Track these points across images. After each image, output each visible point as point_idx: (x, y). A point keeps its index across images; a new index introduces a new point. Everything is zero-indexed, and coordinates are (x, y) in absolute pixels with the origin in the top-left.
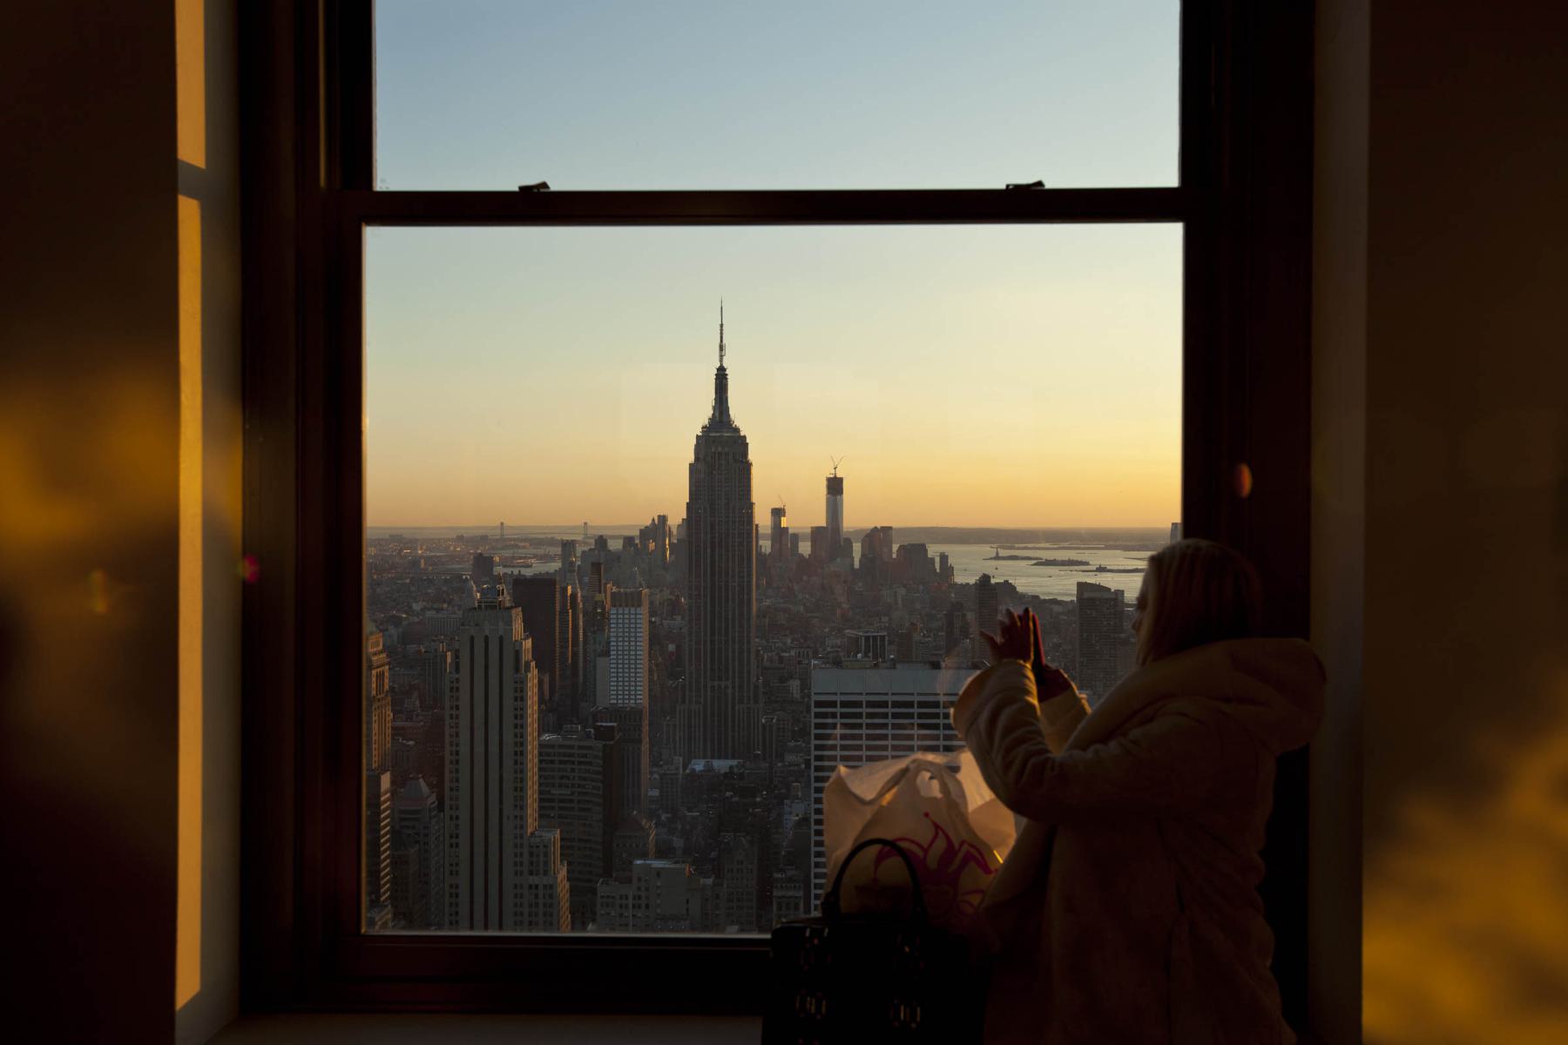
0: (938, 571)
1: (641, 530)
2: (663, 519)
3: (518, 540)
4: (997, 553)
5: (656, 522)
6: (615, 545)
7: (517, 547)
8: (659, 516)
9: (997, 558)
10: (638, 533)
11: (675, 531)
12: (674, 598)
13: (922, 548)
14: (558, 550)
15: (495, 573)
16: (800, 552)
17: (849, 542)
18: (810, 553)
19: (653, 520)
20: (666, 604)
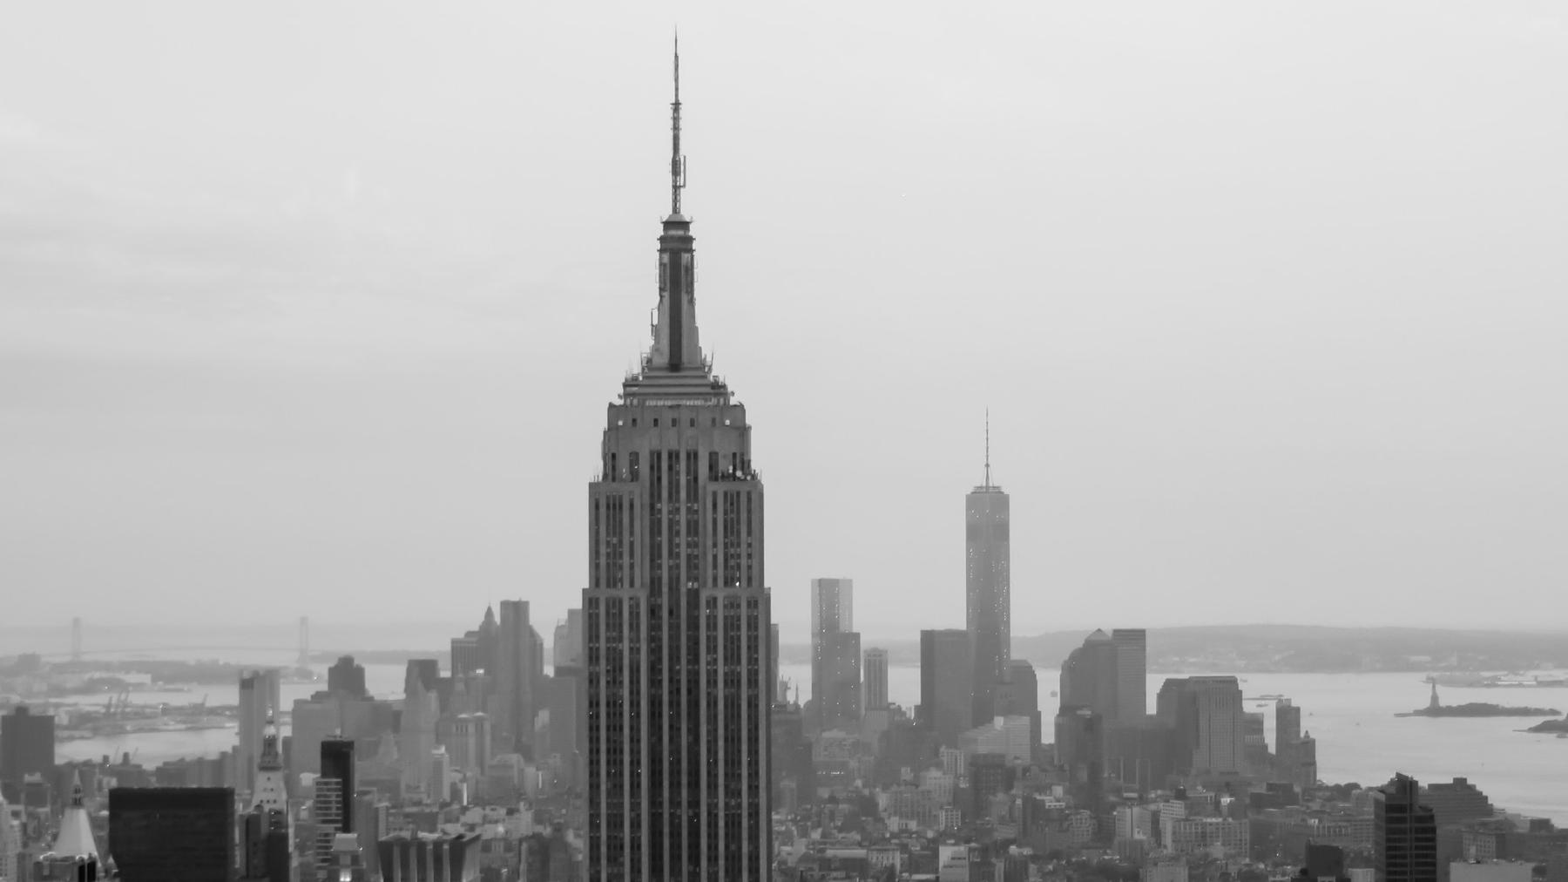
0: (1272, 749)
1: (454, 642)
2: (516, 611)
3: (127, 667)
4: (1435, 698)
5: (497, 619)
6: (385, 684)
7: (121, 686)
8: (505, 605)
9: (1435, 711)
10: (448, 648)
11: (548, 642)
12: (547, 831)
13: (1227, 691)
14: (230, 696)
15: (59, 760)
16: (890, 700)
17: (1025, 678)
18: (917, 700)
19: (489, 613)
20: (524, 846)
